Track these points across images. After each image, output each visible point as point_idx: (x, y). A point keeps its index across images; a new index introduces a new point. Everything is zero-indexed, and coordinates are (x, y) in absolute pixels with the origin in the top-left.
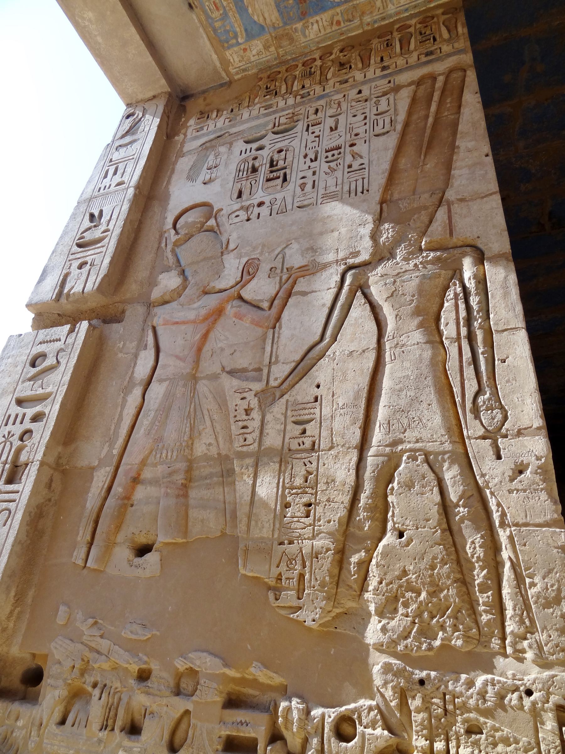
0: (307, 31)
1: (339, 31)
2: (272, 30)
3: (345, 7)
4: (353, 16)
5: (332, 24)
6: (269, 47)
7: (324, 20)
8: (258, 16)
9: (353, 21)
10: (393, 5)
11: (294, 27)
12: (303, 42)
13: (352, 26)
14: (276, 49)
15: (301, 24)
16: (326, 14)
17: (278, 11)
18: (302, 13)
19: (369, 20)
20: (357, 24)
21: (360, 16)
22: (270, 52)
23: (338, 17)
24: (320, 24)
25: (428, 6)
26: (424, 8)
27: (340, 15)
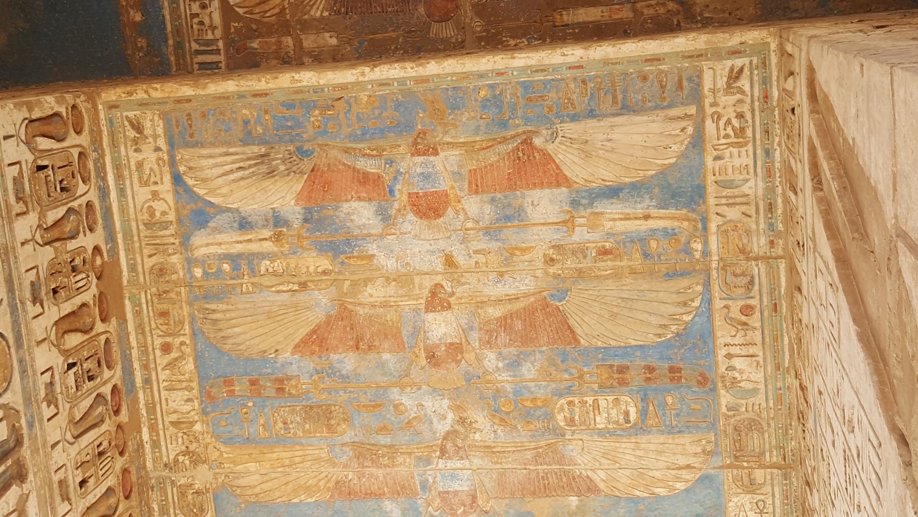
0: (742, 384)
1: (766, 313)
2: (717, 461)
3: (717, 288)
4: (743, 274)
5: (745, 324)
6: (752, 482)
7: (729, 340)
8: (678, 479)
9: (752, 277)
10: (747, 181)
11: (724, 409)
12: (767, 400)
13: (764, 280)
14: (760, 467)
15: (723, 392)
16: (719, 334)
17: (680, 432)
18: (699, 382)
19: (763, 241)
20: (763, 270)
21: (748, 259)
22: (764, 484)
23: (732, 309)
24: (735, 350)
25: (775, 104)
26: (776, 113)
27: (730, 303)
